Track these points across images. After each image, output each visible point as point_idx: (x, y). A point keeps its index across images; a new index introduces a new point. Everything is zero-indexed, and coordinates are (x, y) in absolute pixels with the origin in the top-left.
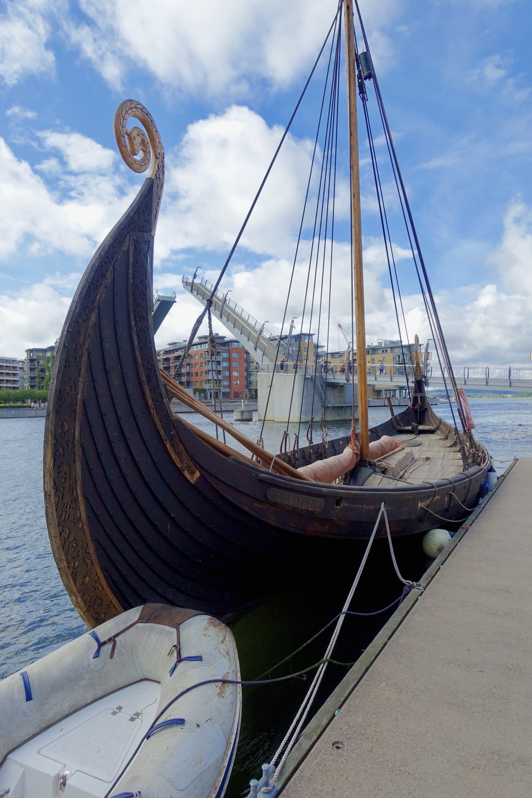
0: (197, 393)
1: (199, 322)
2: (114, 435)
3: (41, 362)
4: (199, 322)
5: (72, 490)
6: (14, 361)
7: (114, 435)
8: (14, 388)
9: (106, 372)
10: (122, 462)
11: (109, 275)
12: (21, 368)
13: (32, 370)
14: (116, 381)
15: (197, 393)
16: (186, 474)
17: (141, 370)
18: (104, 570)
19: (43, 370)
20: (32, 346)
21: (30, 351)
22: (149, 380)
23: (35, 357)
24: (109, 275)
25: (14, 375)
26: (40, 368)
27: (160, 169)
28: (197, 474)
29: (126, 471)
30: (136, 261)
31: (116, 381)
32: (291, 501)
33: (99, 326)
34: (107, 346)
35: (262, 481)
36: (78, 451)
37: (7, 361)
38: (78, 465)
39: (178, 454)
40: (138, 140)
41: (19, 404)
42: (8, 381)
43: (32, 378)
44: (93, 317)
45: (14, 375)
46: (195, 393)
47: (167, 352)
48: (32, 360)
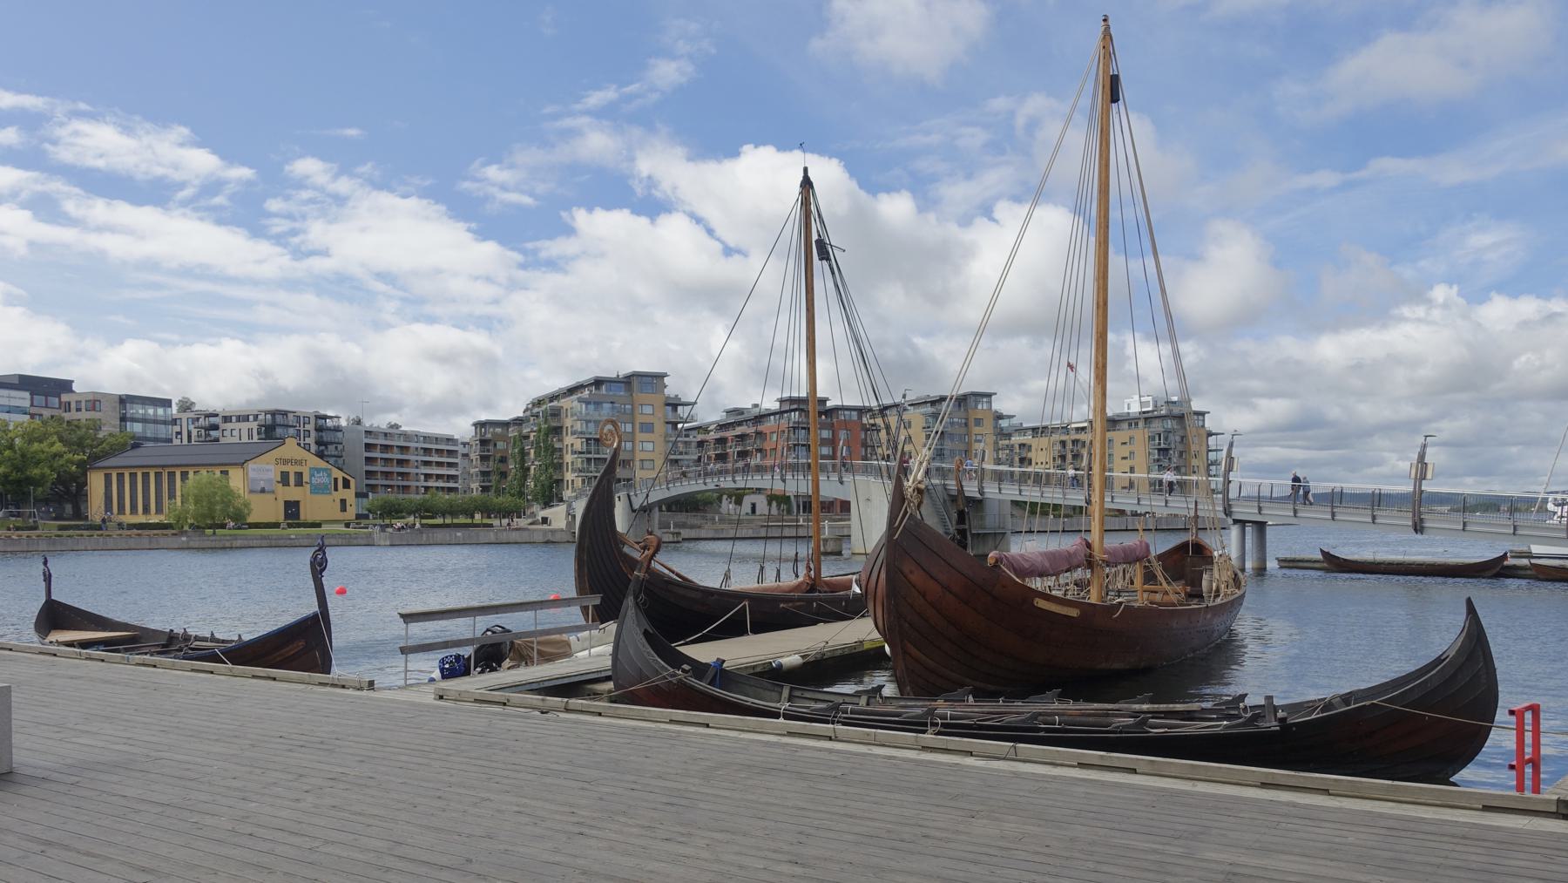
0: (774, 504)
3: (501, 445)
6: (450, 440)
8: (450, 490)
12: (465, 455)
13: (484, 458)
15: (774, 504)
19: (503, 460)
20: (484, 417)
21: (480, 425)
23: (489, 436)
25: (450, 465)
26: (498, 456)
37: (437, 439)
41: (462, 520)
42: (439, 477)
43: (484, 474)
45: (450, 465)
46: (770, 504)
47: (722, 427)
48: (484, 442)
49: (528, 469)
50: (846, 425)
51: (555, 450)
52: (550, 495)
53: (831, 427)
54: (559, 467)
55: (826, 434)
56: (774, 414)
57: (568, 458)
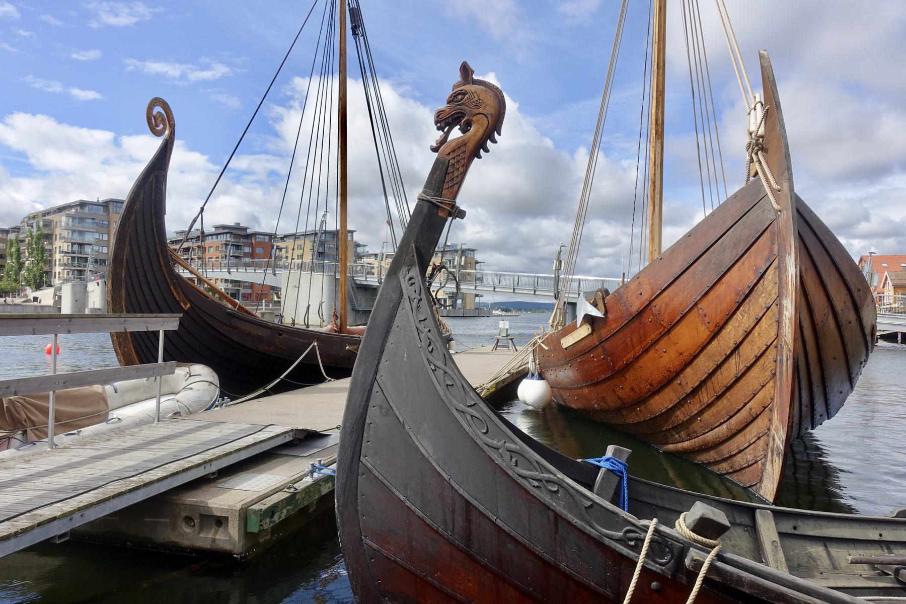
1: (195, 221)
2: (142, 278)
4: (195, 221)
5: (120, 303)
7: (142, 278)
9: (139, 246)
10: (146, 293)
11: (142, 196)
14: (144, 251)
16: (182, 304)
17: (158, 246)
18: (134, 347)
22: (162, 252)
24: (142, 196)
27: (172, 133)
28: (189, 305)
29: (148, 298)
30: (156, 187)
31: (144, 251)
32: (247, 327)
33: (136, 222)
34: (139, 232)
35: (228, 314)
36: (123, 284)
38: (123, 291)
39: (178, 293)
40: (160, 119)
44: (133, 217)
49: (24, 263)
50: (260, 244)
51: (43, 250)
52: (41, 281)
53: (251, 245)
54: (50, 262)
55: (247, 250)
56: (212, 235)
57: (58, 256)
